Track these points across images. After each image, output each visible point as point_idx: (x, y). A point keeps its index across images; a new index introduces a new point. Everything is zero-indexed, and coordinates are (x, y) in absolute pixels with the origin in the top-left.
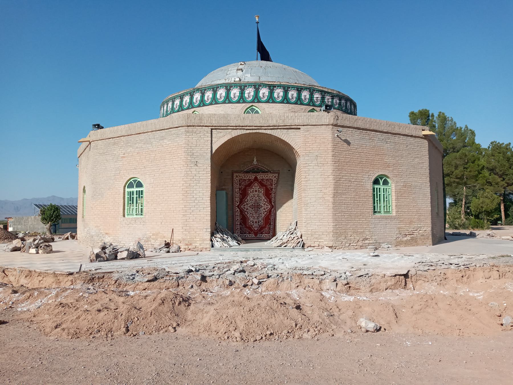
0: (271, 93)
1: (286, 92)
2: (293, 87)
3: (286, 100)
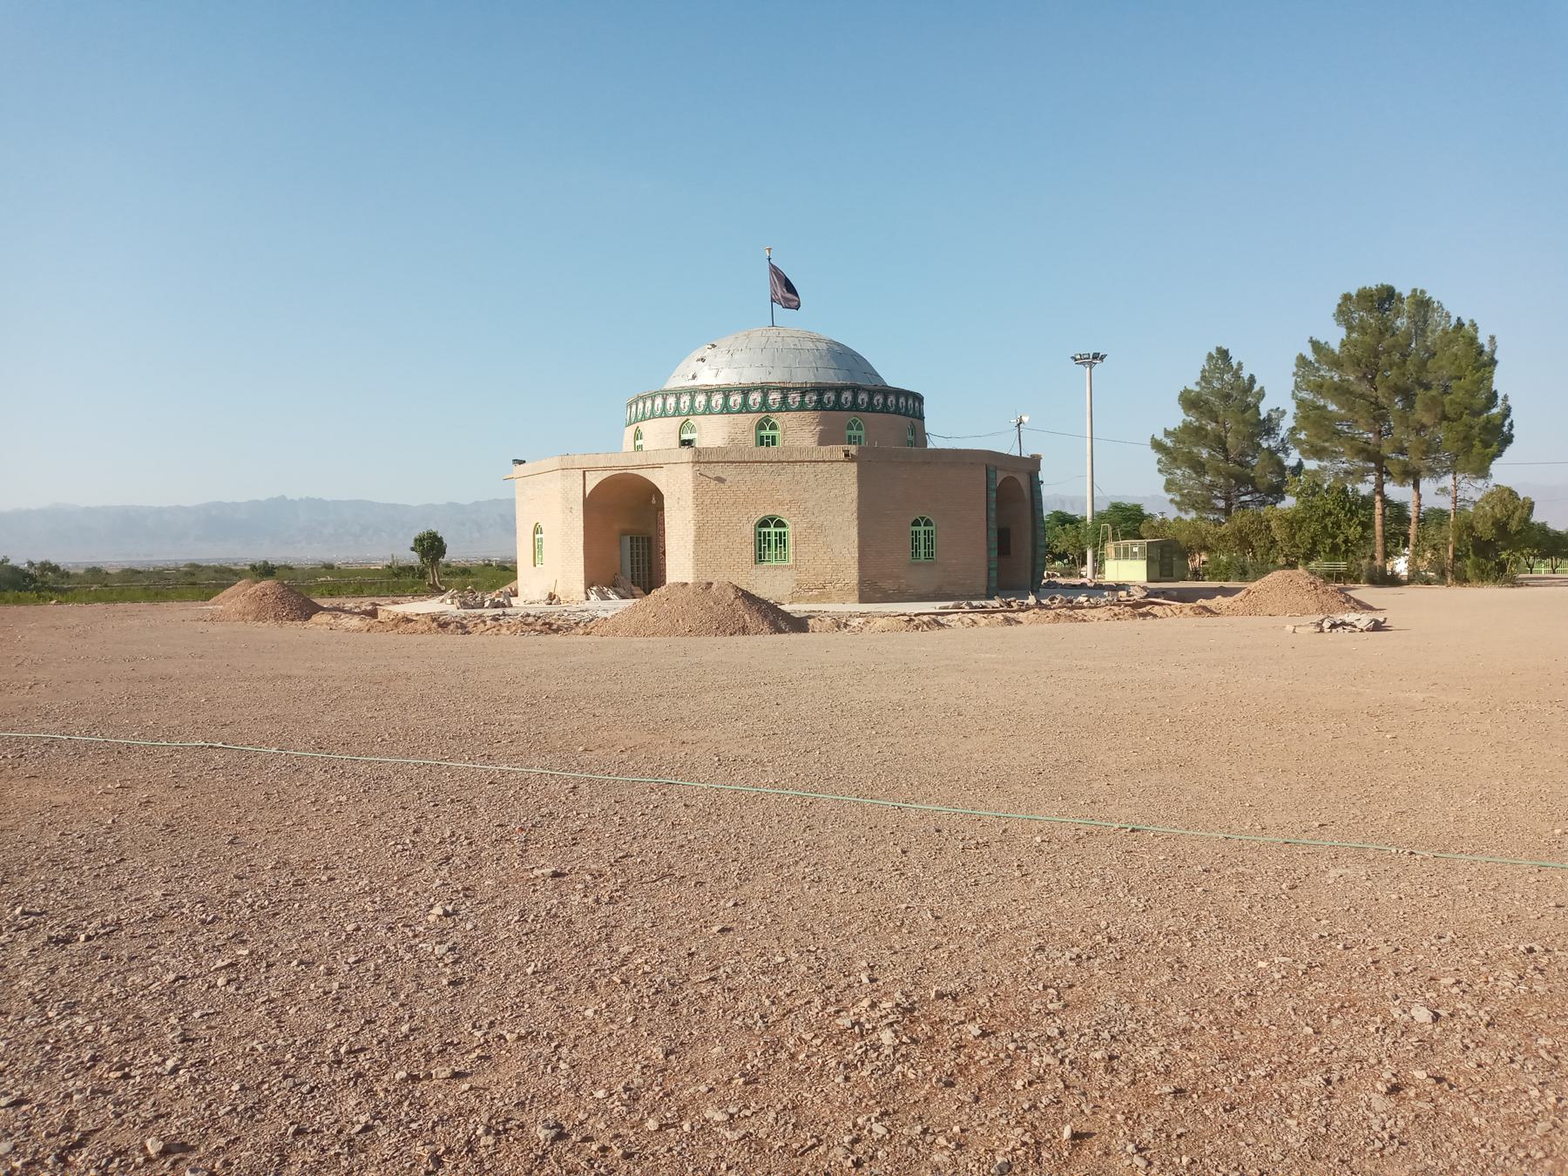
0: (709, 401)
1: (726, 398)
2: (736, 389)
3: (726, 409)
